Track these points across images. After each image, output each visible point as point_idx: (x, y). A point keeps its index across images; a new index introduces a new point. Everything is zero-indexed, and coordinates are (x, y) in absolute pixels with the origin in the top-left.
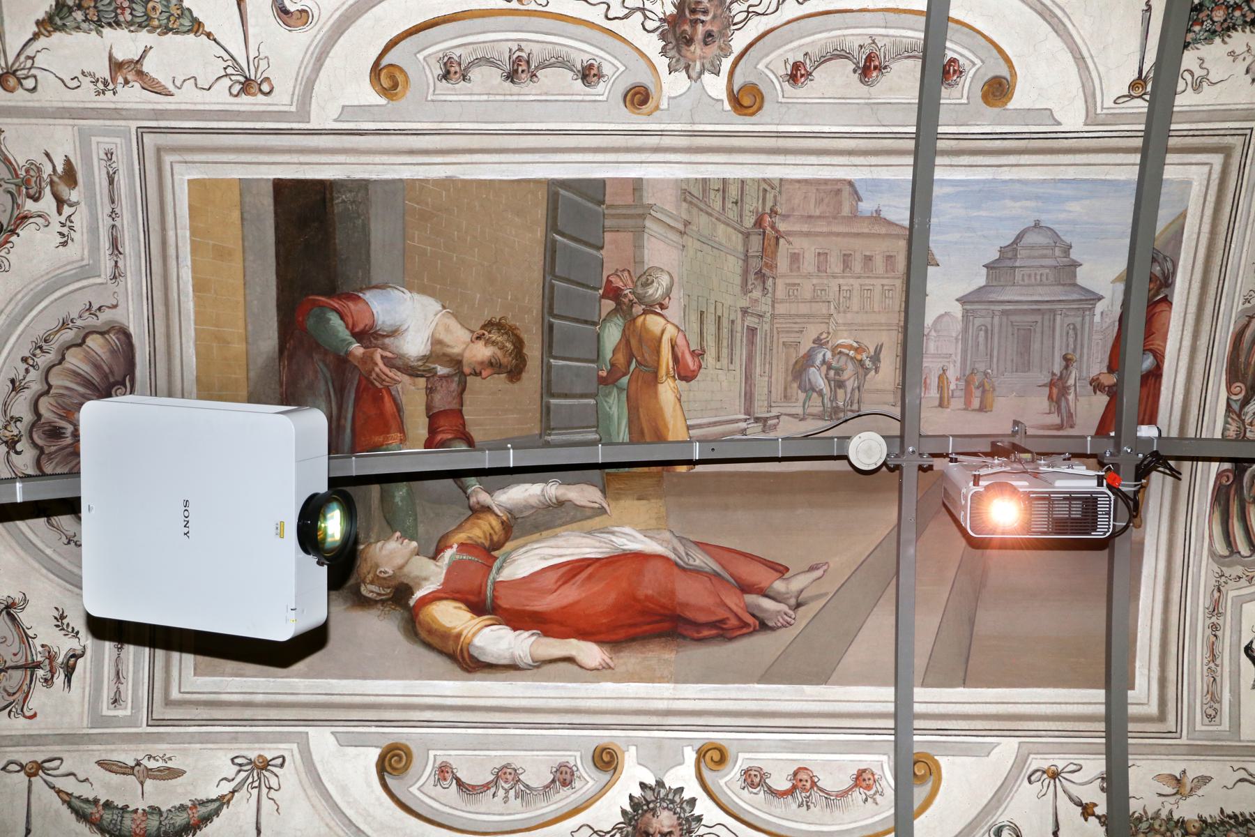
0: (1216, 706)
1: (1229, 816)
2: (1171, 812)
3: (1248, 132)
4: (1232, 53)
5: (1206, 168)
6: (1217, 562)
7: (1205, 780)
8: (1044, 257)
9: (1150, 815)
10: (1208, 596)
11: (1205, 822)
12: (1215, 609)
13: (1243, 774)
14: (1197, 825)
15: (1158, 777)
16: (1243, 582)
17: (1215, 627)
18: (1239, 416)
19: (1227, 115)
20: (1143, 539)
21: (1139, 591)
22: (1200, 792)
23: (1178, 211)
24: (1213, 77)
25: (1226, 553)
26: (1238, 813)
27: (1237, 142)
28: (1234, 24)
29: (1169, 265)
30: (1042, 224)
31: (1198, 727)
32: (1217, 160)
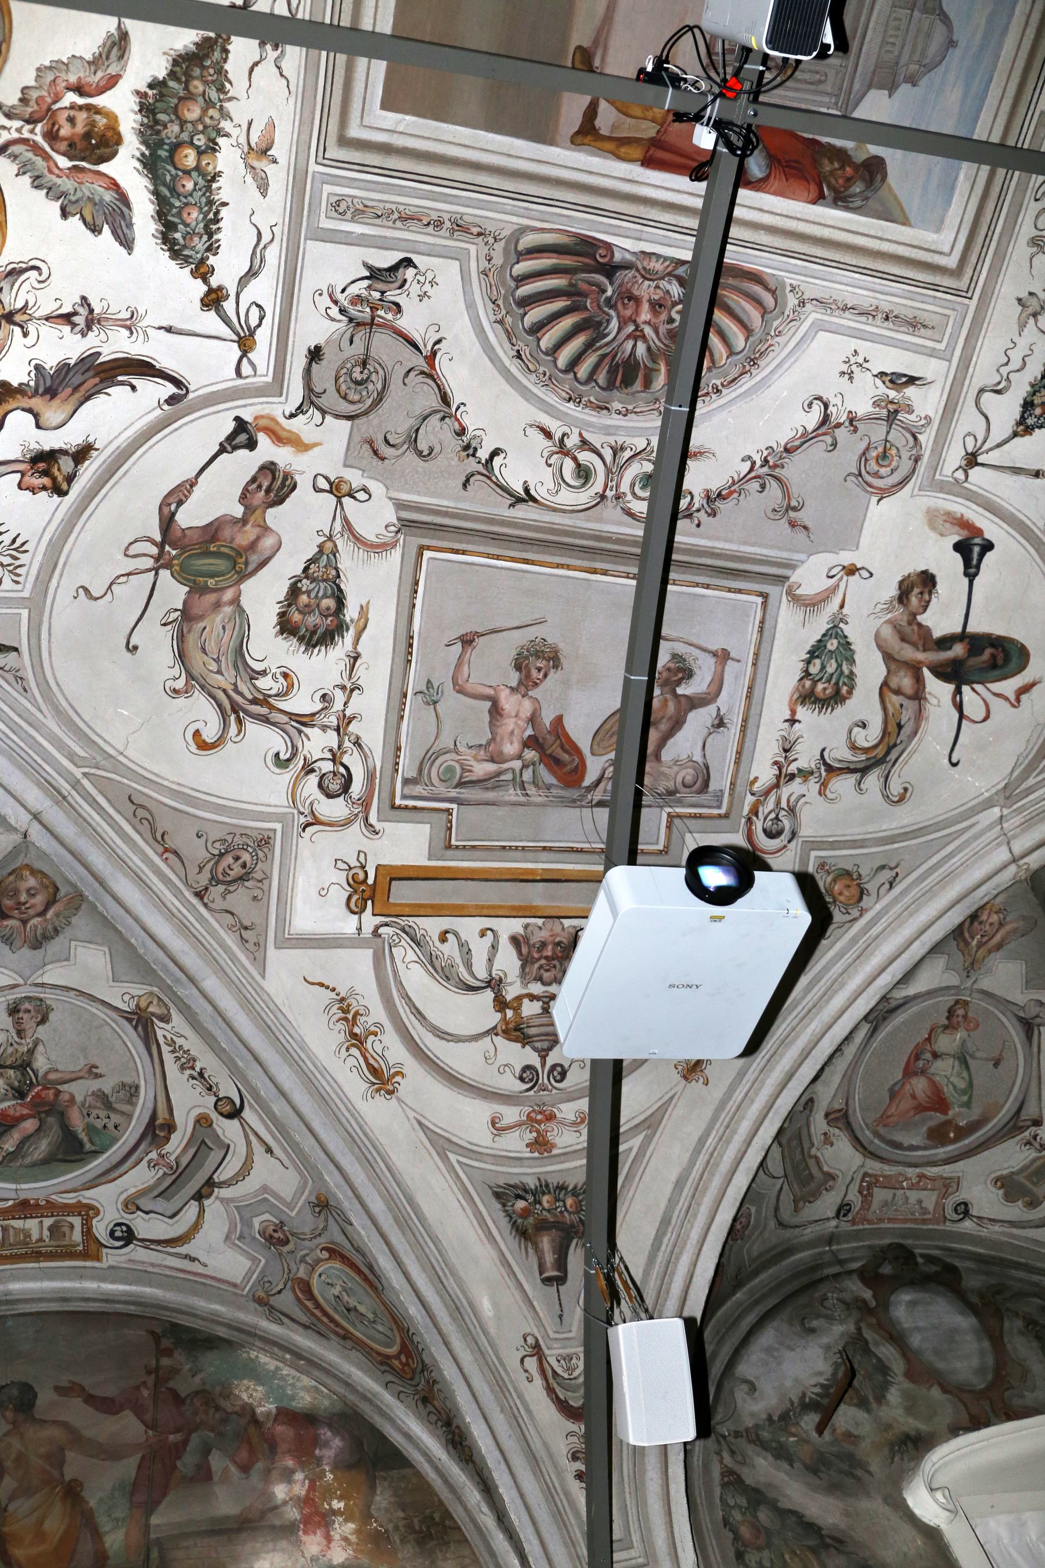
0: (349, 215)
1: (217, 213)
2: (227, 135)
5: (946, 249)
6: (512, 234)
7: (263, 187)
9: (226, 105)
10: (477, 220)
11: (213, 179)
12: (459, 227)
13: (266, 237)
14: (210, 168)
15: (271, 125)
16: (484, 264)
17: (438, 224)
18: (669, 274)
20: (557, 146)
21: (496, 133)
22: (249, 178)
25: (520, 248)
26: (221, 224)
27: (963, 284)
29: (858, 203)
31: (327, 189)
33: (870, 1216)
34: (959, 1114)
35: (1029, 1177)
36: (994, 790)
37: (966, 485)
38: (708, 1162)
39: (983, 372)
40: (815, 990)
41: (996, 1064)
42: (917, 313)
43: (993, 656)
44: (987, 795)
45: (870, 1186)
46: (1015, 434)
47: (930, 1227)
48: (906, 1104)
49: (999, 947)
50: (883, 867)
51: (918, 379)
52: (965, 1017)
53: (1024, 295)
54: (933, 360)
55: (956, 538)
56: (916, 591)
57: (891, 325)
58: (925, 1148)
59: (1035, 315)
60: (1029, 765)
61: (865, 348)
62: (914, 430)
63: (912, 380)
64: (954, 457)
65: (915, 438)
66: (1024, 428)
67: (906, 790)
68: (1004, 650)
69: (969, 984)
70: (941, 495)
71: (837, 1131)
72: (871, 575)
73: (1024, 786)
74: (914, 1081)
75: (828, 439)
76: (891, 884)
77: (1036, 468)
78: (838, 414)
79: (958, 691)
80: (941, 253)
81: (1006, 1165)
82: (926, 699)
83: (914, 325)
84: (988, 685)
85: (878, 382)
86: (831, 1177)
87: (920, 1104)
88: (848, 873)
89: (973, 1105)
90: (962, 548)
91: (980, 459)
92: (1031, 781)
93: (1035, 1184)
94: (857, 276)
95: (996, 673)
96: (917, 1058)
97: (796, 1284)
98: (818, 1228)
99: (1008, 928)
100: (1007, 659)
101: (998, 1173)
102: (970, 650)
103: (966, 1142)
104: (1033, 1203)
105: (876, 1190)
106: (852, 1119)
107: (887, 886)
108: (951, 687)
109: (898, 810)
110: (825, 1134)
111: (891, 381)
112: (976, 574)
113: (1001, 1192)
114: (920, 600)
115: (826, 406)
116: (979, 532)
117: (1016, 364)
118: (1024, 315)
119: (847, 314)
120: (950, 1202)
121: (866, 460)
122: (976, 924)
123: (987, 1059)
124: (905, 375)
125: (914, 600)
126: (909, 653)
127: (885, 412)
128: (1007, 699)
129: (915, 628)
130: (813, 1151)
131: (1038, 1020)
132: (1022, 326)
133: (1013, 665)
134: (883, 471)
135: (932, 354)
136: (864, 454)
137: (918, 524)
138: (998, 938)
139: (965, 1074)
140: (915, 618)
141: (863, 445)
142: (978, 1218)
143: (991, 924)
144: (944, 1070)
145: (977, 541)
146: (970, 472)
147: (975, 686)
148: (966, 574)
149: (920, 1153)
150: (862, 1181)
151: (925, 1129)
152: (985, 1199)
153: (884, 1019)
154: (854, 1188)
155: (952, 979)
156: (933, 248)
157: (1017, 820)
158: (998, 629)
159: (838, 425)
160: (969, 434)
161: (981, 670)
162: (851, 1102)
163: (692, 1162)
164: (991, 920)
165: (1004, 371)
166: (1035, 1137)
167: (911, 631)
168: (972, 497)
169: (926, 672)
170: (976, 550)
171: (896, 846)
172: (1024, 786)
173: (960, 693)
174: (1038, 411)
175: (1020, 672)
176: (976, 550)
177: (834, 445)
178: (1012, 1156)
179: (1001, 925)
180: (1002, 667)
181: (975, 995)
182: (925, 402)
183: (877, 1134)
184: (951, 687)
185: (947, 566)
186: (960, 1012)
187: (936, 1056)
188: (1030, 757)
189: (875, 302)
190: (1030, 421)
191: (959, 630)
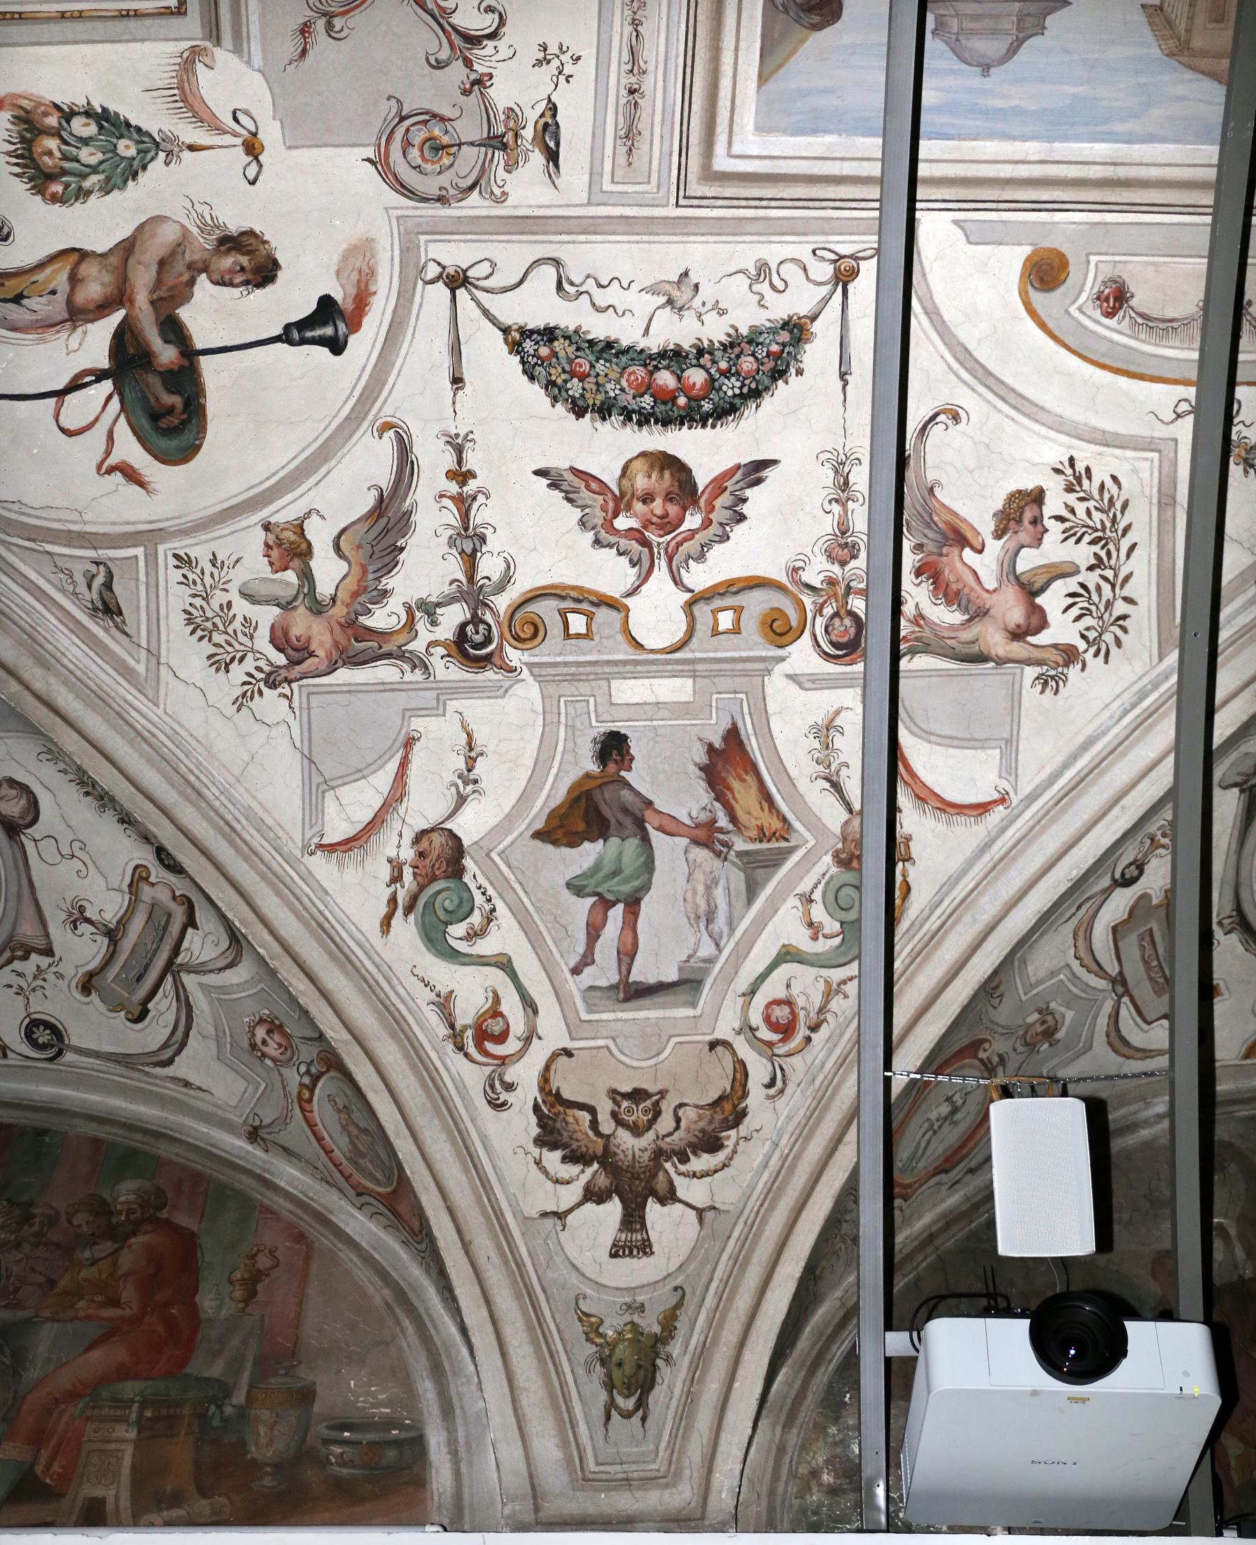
3: (682, 202)
4: (722, 312)
5: (736, 149)
8: (976, 17)
19: (718, 228)
23: (771, 86)
24: (742, 281)
27: (695, 188)
28: (725, 350)
30: (978, 70)
32: (721, 163)
37: (420, 283)
39: (583, 257)
42: (646, 133)
43: (170, 410)
46: (506, 331)
51: (557, 166)
53: (694, 278)
54: (587, 176)
55: (338, 296)
56: (244, 260)
57: (624, 101)
59: (670, 302)
61: (585, 73)
62: (483, 182)
63: (553, 156)
64: (455, 254)
65: (472, 188)
66: (517, 339)
68: (184, 423)
70: (397, 252)
72: (252, 183)
75: (444, 54)
77: (466, 377)
78: (486, 58)
79: (100, 376)
80: (730, 143)
82: (75, 328)
83: (630, 135)
84: (122, 419)
85: (541, 107)
90: (326, 308)
91: (461, 293)
94: (683, 27)
95: (145, 423)
100: (171, 432)
102: (171, 372)
108: (104, 363)
111: (546, 125)
112: (291, 343)
114: (231, 271)
115: (493, 36)
116: (355, 326)
117: (601, 298)
118: (668, 287)
119: (629, 29)
121: (425, 122)
124: (558, 144)
125: (228, 262)
126: (142, 281)
127: (501, 129)
128: (108, 453)
129: (186, 277)
132: (653, 290)
133: (164, 443)
134: (414, 153)
135: (594, 175)
136: (434, 116)
137: (347, 232)
140: (200, 271)
141: (446, 111)
145: (342, 328)
146: (440, 284)
147: (116, 398)
148: (288, 327)
156: (735, 128)
158: (213, 404)
159: (468, 63)
160: (494, 265)
161: (144, 398)
165: (590, 285)
167: (179, 270)
168: (405, 299)
169: (119, 315)
170: (328, 331)
173: (98, 380)
174: (544, 351)
175: (156, 457)
176: (328, 331)
177: (439, 65)
180: (157, 429)
182: (526, 187)
184: (104, 363)
185: (293, 297)
189: (651, 68)
190: (528, 345)
191: (199, 345)
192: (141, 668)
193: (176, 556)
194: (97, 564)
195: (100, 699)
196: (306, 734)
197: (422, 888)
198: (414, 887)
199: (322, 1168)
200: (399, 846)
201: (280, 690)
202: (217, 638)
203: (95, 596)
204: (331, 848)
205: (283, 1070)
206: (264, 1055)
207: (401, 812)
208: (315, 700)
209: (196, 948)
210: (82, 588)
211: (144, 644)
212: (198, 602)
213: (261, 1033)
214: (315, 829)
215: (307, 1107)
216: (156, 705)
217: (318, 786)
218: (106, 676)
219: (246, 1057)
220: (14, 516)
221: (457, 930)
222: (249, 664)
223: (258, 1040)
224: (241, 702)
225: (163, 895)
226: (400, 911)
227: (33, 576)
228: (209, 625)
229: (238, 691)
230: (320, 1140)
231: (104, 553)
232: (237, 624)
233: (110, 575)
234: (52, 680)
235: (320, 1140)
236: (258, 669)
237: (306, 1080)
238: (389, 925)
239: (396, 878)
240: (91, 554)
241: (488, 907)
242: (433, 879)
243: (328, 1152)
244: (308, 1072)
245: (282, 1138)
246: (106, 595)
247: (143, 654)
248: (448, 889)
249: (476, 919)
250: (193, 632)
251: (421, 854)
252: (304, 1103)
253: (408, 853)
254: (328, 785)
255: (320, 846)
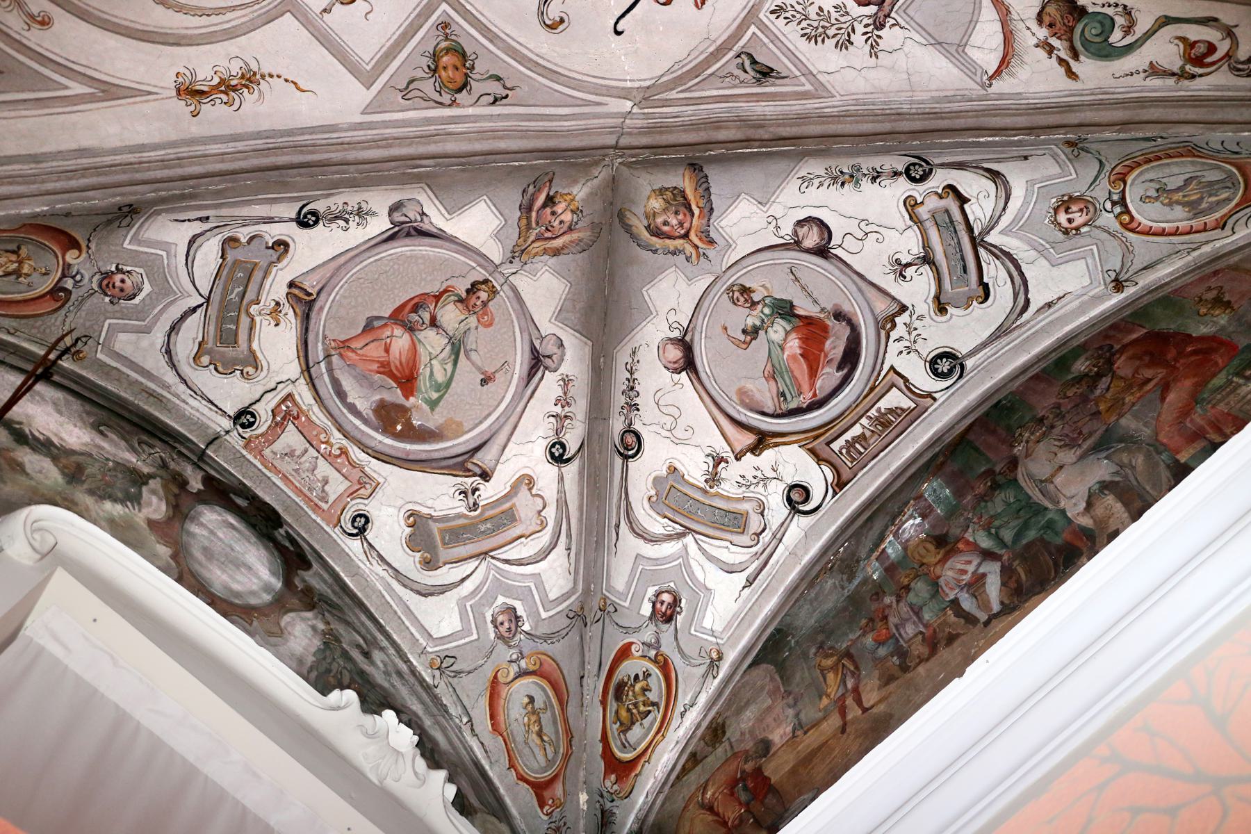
33: (267, 452)
34: (417, 407)
35: (441, 531)
36: (637, 85)
38: (131, 164)
40: (362, 133)
41: (484, 382)
44: (629, 84)
45: (288, 413)
47: (319, 520)
48: (375, 351)
49: (556, 252)
50: (498, 79)
52: (485, 304)
58: (366, 421)
60: (680, 77)
67: (562, 21)
69: (507, 269)
71: (291, 312)
73: (663, 96)
74: (398, 331)
76: (496, 100)
81: (430, 503)
86: (254, 360)
87: (389, 363)
88: (463, 55)
89: (438, 409)
92: (673, 95)
93: (444, 544)
96: (415, 309)
97: (136, 420)
98: (206, 411)
99: (574, 236)
101: (417, 508)
103: (408, 447)
104: (430, 564)
105: (291, 426)
106: (313, 315)
107: (491, 99)
109: (543, 33)
110: (278, 304)
113: (408, 530)
120: (355, 506)
122: (548, 210)
123: (479, 369)
130: (254, 309)
131: (548, 362)
138: (558, 243)
139: (449, 367)
142: (370, 545)
143: (561, 222)
144: (432, 342)
149: (358, 422)
150: (284, 401)
151: (378, 397)
152: (389, 530)
153: (408, 235)
154: (271, 401)
155: (495, 253)
157: (639, 123)
162: (323, 295)
163: (115, 151)
164: (563, 217)
166: (475, 490)
171: (522, 68)
172: (663, 96)
178: (440, 495)
179: (570, 229)
181: (506, 287)
183: (328, 356)
186: (484, 295)
187: (434, 323)
188: (685, 69)
192: (808, 87)
193: (773, 12)
194: (739, 56)
195: (804, 118)
196: (924, 33)
197: (1071, 40)
198: (1066, 44)
199: (1181, 247)
200: (1034, 34)
201: (888, 25)
202: (831, 32)
203: (752, 73)
204: (998, 73)
205: (1097, 223)
206: (1077, 229)
207: (1015, 16)
208: (911, 11)
209: (980, 214)
210: (743, 75)
211: (798, 73)
212: (804, 24)
213: (1062, 218)
214: (979, 73)
215: (1134, 225)
216: (833, 96)
217: (956, 50)
218: (796, 106)
219: (1068, 244)
220: (680, 72)
221: (1116, 37)
222: (860, 29)
223: (1065, 224)
224: (874, 53)
225: (933, 203)
226: (1072, 62)
227: (715, 93)
228: (821, 30)
229: (868, 48)
230: (1162, 233)
231: (737, 48)
232: (834, 15)
233: (750, 56)
234: (771, 129)
235: (1162, 233)
236: (867, 26)
237: (1118, 209)
238: (1074, 73)
239: (1051, 50)
240: (731, 54)
241: (1120, 9)
242: (1072, 29)
243: (1176, 233)
244: (1114, 203)
245: (1138, 265)
246: (757, 67)
247: (803, 79)
248: (1085, 25)
249: (1120, 21)
250: (816, 42)
251: (1051, 26)
252: (1130, 226)
253: (1042, 33)
254: (962, 46)
255: (991, 78)
